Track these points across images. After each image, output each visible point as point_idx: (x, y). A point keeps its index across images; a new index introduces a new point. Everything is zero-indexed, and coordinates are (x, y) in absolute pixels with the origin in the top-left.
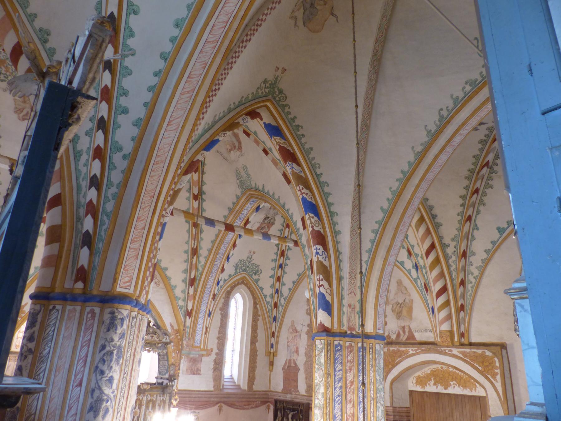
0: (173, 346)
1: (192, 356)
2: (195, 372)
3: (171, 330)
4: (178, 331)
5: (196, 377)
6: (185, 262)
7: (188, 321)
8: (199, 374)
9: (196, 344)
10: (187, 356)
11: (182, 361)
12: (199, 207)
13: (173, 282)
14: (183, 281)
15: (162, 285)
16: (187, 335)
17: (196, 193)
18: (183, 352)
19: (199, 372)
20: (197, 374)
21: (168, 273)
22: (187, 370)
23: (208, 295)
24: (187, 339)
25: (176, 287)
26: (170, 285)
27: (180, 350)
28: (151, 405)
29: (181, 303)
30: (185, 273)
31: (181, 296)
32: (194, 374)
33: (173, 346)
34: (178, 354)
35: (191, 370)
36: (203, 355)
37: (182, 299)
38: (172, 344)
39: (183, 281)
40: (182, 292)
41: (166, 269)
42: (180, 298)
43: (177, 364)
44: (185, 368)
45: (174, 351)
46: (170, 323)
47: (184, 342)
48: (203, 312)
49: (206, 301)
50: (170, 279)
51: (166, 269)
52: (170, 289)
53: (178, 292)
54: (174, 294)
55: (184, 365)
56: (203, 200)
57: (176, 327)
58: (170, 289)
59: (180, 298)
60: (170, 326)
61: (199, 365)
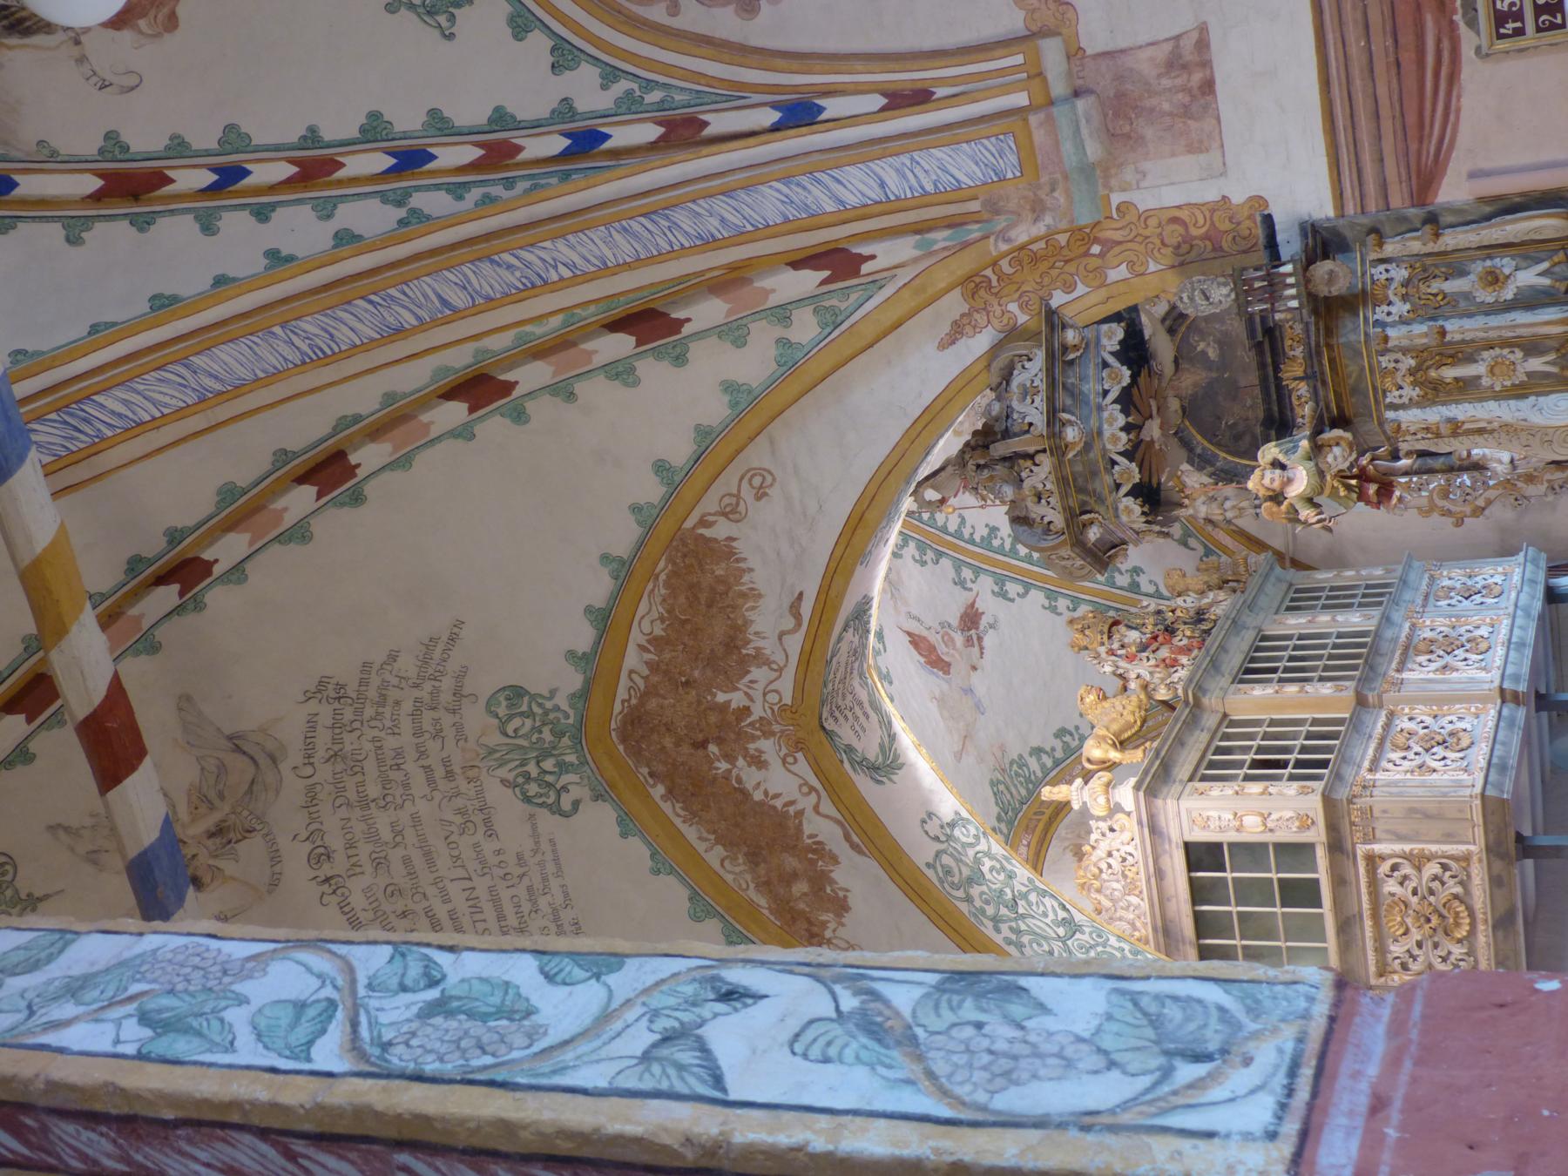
0: (1069, 288)
1: (1094, 150)
2: (1197, 77)
3: (977, 329)
4: (973, 285)
5: (1227, 68)
6: (571, 396)
7: (886, 253)
8: (1203, 44)
9: (1009, 164)
10: (1096, 175)
11: (1145, 200)
12: (230, 526)
13: (716, 410)
14: (680, 360)
15: (757, 455)
16: (974, 232)
17: (168, 595)
18: (1085, 218)
19: (1188, 44)
20: (1206, 64)
21: (680, 451)
22: (1196, 147)
23: (680, 217)
24: (1001, 222)
25: (729, 387)
26: (737, 419)
27: (1081, 246)
28: (1449, 373)
29: (805, 328)
30: (633, 370)
31: (763, 336)
32: (1208, 86)
33: (1069, 288)
34: (1109, 245)
35: (1186, 112)
36: (1074, 53)
37: (779, 332)
38: (1058, 299)
39: (680, 360)
40: (740, 342)
41: (661, 467)
42: (783, 342)
43: (1173, 234)
44: (1188, 164)
45: (1097, 276)
46: (944, 345)
47: (1021, 234)
48: (797, 194)
49: (721, 205)
50: (703, 433)
51: (661, 467)
52: (755, 413)
53: (753, 363)
54: (772, 385)
55: (1169, 184)
56: (174, 536)
57: (954, 304)
58: (755, 413)
59: (783, 342)
60: (962, 344)
61: (1145, 64)
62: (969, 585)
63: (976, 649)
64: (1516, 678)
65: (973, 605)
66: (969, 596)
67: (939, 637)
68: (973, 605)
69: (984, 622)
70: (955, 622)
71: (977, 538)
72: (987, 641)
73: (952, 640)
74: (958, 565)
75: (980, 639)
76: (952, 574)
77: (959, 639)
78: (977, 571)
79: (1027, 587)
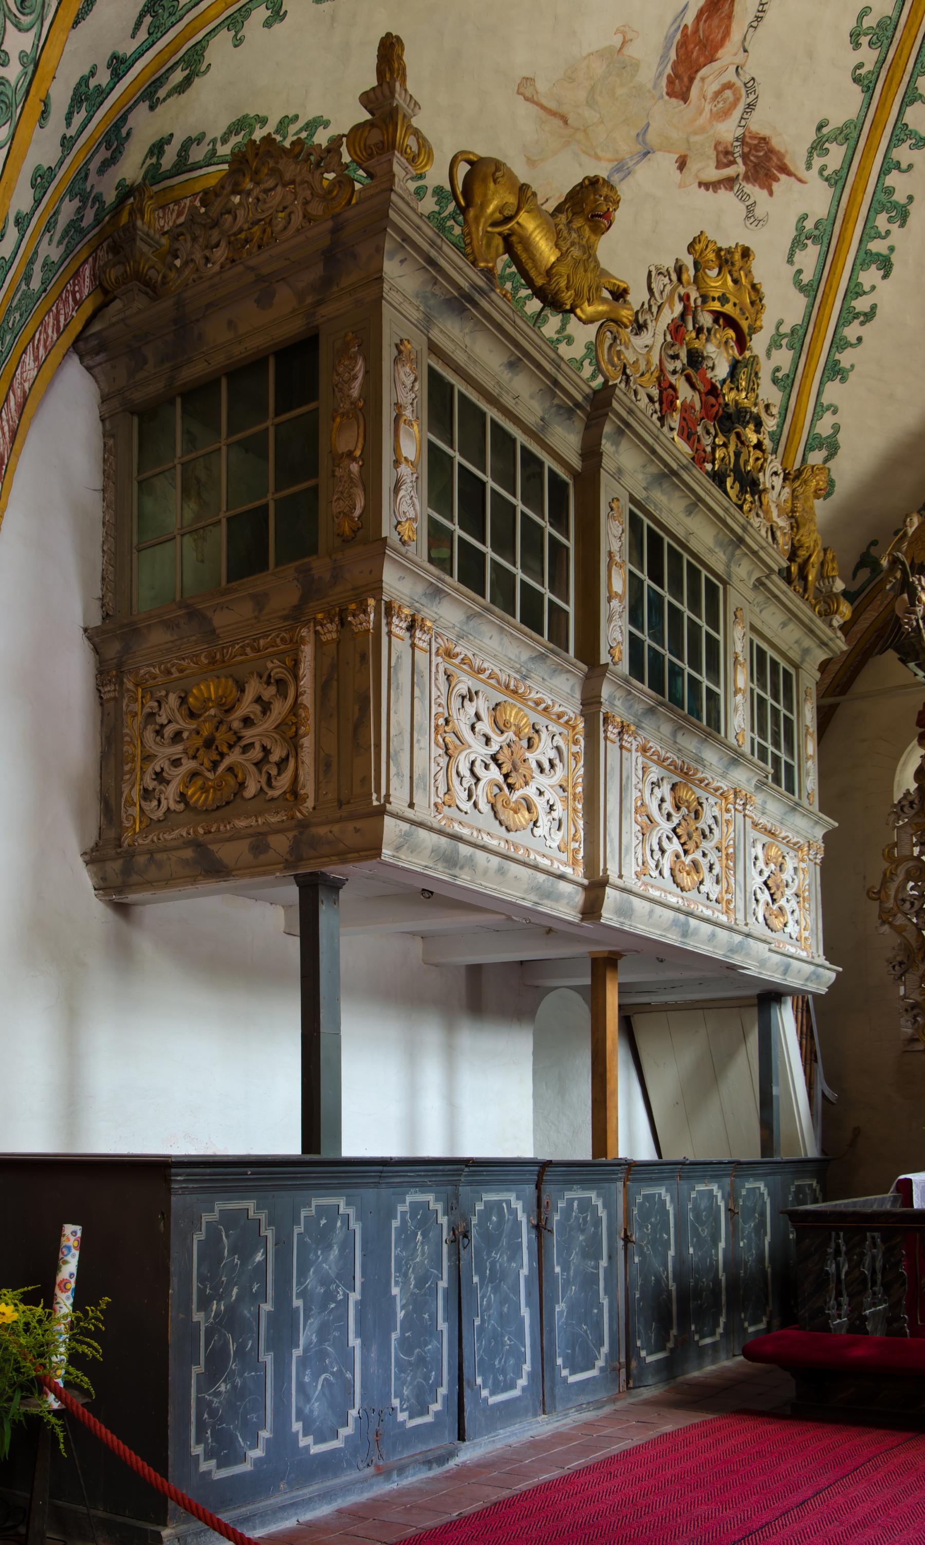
62: (817, 162)
63: (713, 174)
64: (624, 911)
65: (784, 170)
66: (796, 157)
67: (730, 76)
68: (784, 170)
69: (755, 192)
70: (758, 124)
71: (893, 179)
72: (725, 197)
73: (725, 113)
74: (847, 134)
75: (729, 183)
76: (837, 120)
77: (728, 130)
78: (836, 180)
79: (808, 289)
